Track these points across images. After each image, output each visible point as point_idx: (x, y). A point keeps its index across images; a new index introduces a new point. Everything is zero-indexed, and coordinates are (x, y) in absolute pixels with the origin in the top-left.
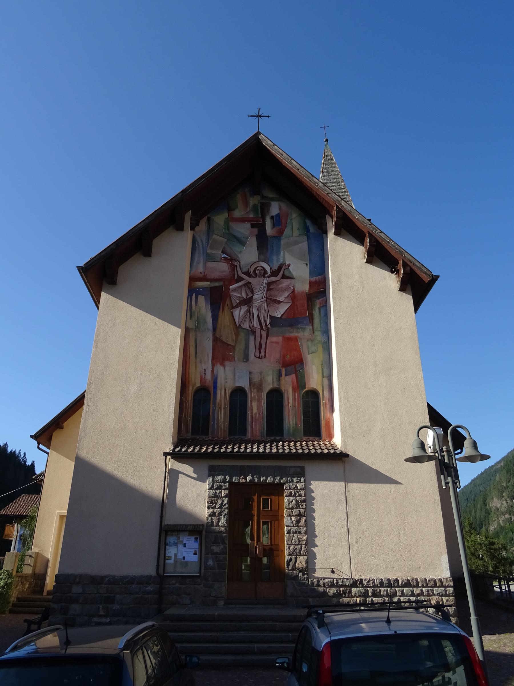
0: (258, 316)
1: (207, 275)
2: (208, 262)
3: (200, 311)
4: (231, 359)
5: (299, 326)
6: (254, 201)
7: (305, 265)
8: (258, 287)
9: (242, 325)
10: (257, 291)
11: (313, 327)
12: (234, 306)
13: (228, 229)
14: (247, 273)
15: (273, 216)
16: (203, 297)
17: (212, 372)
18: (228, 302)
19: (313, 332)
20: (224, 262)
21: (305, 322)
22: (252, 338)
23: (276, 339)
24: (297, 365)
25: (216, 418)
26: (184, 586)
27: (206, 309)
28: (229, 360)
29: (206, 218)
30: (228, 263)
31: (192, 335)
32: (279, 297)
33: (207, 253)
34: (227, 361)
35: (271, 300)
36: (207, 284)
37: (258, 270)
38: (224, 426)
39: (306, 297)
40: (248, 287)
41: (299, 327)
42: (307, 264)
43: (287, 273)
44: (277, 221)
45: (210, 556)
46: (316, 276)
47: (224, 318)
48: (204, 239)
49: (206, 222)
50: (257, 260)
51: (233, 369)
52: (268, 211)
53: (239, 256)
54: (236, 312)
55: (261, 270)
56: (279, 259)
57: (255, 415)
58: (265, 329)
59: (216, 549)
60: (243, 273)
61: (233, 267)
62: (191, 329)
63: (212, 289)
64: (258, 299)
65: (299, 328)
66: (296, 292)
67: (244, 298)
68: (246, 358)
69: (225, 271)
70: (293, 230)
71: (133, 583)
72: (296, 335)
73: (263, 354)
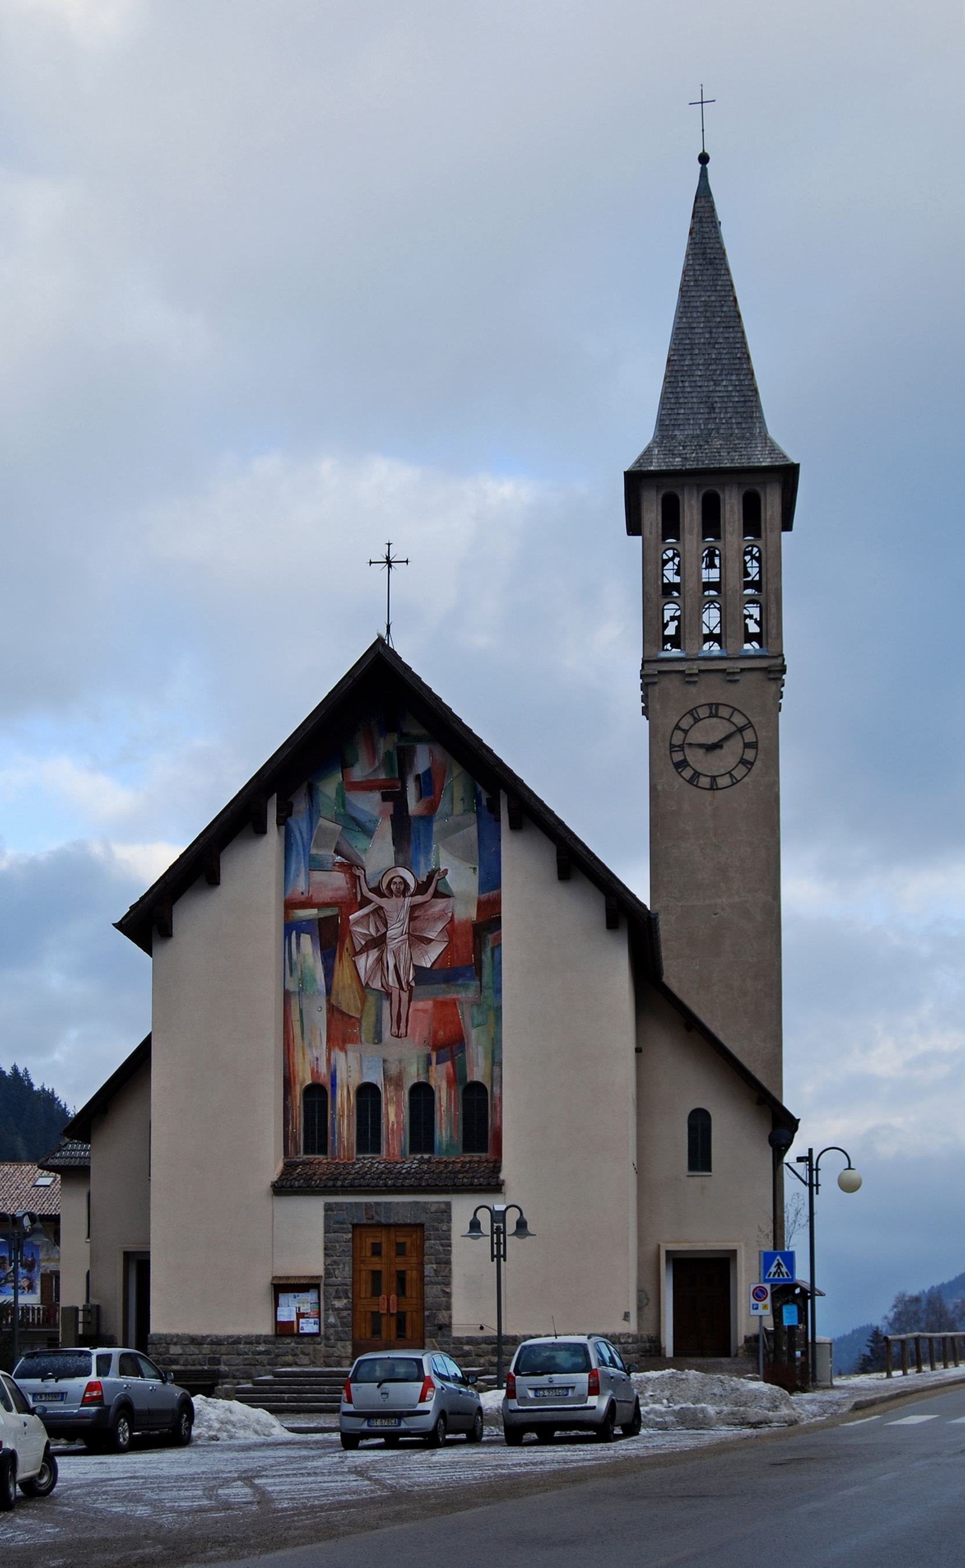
0: (395, 966)
1: (313, 898)
3: (304, 962)
4: (355, 1039)
5: (460, 982)
6: (385, 745)
7: (472, 870)
8: (395, 915)
9: (370, 984)
10: (393, 923)
11: (481, 983)
12: (357, 951)
13: (344, 807)
14: (377, 891)
15: (419, 775)
17: (329, 1060)
20: (339, 871)
21: (468, 974)
22: (386, 1004)
26: (301, 1346)
27: (314, 958)
28: (352, 1041)
29: (305, 784)
30: (345, 873)
32: (429, 931)
34: (349, 1043)
36: (311, 913)
37: (396, 883)
38: (348, 1143)
40: (379, 915)
42: (475, 869)
43: (441, 889)
44: (428, 785)
45: (330, 1312)
47: (343, 973)
48: (304, 826)
49: (305, 795)
51: (359, 1055)
52: (411, 764)
53: (363, 858)
56: (430, 860)
57: (393, 1125)
58: (406, 989)
59: (338, 1304)
62: (293, 992)
63: (322, 921)
65: (459, 986)
66: (456, 921)
68: (378, 1038)
70: (452, 803)
71: (240, 1343)
72: (455, 996)
73: (403, 1030)
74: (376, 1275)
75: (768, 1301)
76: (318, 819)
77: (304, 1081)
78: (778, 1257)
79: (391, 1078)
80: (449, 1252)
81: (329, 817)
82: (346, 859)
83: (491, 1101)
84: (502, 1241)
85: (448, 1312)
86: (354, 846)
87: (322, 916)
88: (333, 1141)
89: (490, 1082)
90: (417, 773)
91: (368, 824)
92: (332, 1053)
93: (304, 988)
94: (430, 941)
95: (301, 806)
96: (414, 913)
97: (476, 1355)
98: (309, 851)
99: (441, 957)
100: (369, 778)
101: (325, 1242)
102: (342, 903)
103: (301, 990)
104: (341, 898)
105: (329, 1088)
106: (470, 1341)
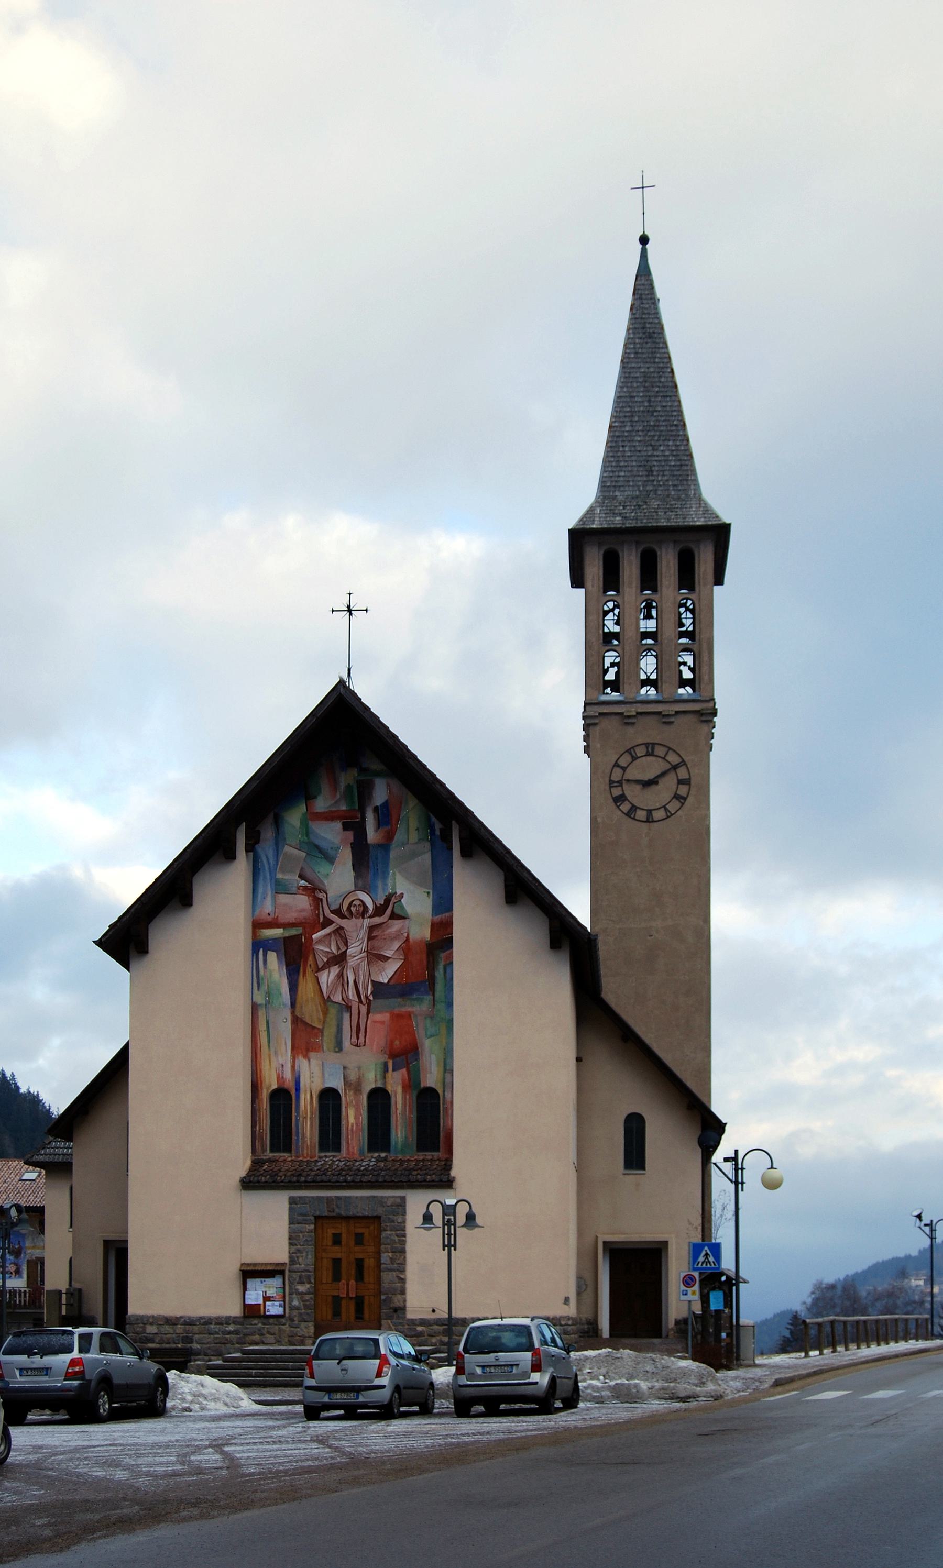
0: (355, 981)
1: (279, 919)
2: (279, 895)
3: (271, 976)
4: (318, 1048)
5: (415, 996)
6: (347, 778)
8: (354, 934)
9: (332, 998)
10: (353, 942)
12: (320, 967)
13: (307, 835)
14: (338, 912)
15: (377, 807)
16: (274, 954)
17: (293, 1067)
18: (311, 960)
19: (434, 1005)
20: (303, 894)
21: (422, 989)
22: (346, 1016)
23: (381, 1017)
24: (409, 1055)
25: (300, 1131)
26: (267, 1326)
29: (272, 815)
30: (309, 896)
31: (262, 1014)
32: (387, 950)
33: (276, 881)
35: (373, 956)
37: (355, 905)
38: (311, 1142)
39: (425, 949)
40: (340, 934)
41: (413, 997)
42: (428, 893)
43: (397, 911)
44: (385, 816)
45: (294, 1296)
46: (442, 913)
47: (306, 988)
48: (271, 854)
50: (353, 889)
51: (321, 1063)
52: (370, 797)
53: (326, 882)
54: (323, 977)
55: (359, 905)
56: (386, 885)
57: (352, 1126)
58: (364, 1003)
59: (301, 1288)
60: (332, 912)
61: (317, 902)
62: (260, 1005)
64: (354, 955)
65: (414, 1000)
66: (411, 940)
67: (333, 953)
68: (339, 1047)
69: (302, 910)
71: (211, 1324)
72: (410, 1009)
73: (361, 1040)
74: (337, 1263)
75: (696, 1287)
76: (284, 847)
77: (270, 1086)
78: (706, 1248)
79: (351, 1083)
80: (403, 1243)
81: (293, 844)
82: (309, 883)
83: (443, 1104)
84: (452, 1232)
85: (403, 1296)
86: (317, 872)
87: (287, 935)
88: (298, 1140)
89: (442, 1086)
90: (375, 805)
91: (330, 851)
92: (296, 1061)
93: (271, 1001)
94: (386, 959)
95: (268, 834)
96: (372, 933)
97: (429, 1335)
98: (276, 876)
99: (398, 973)
100: (331, 809)
101: (289, 1233)
102: (306, 923)
103: (268, 1002)
104: (305, 918)
105: (293, 1092)
106: (423, 1322)
